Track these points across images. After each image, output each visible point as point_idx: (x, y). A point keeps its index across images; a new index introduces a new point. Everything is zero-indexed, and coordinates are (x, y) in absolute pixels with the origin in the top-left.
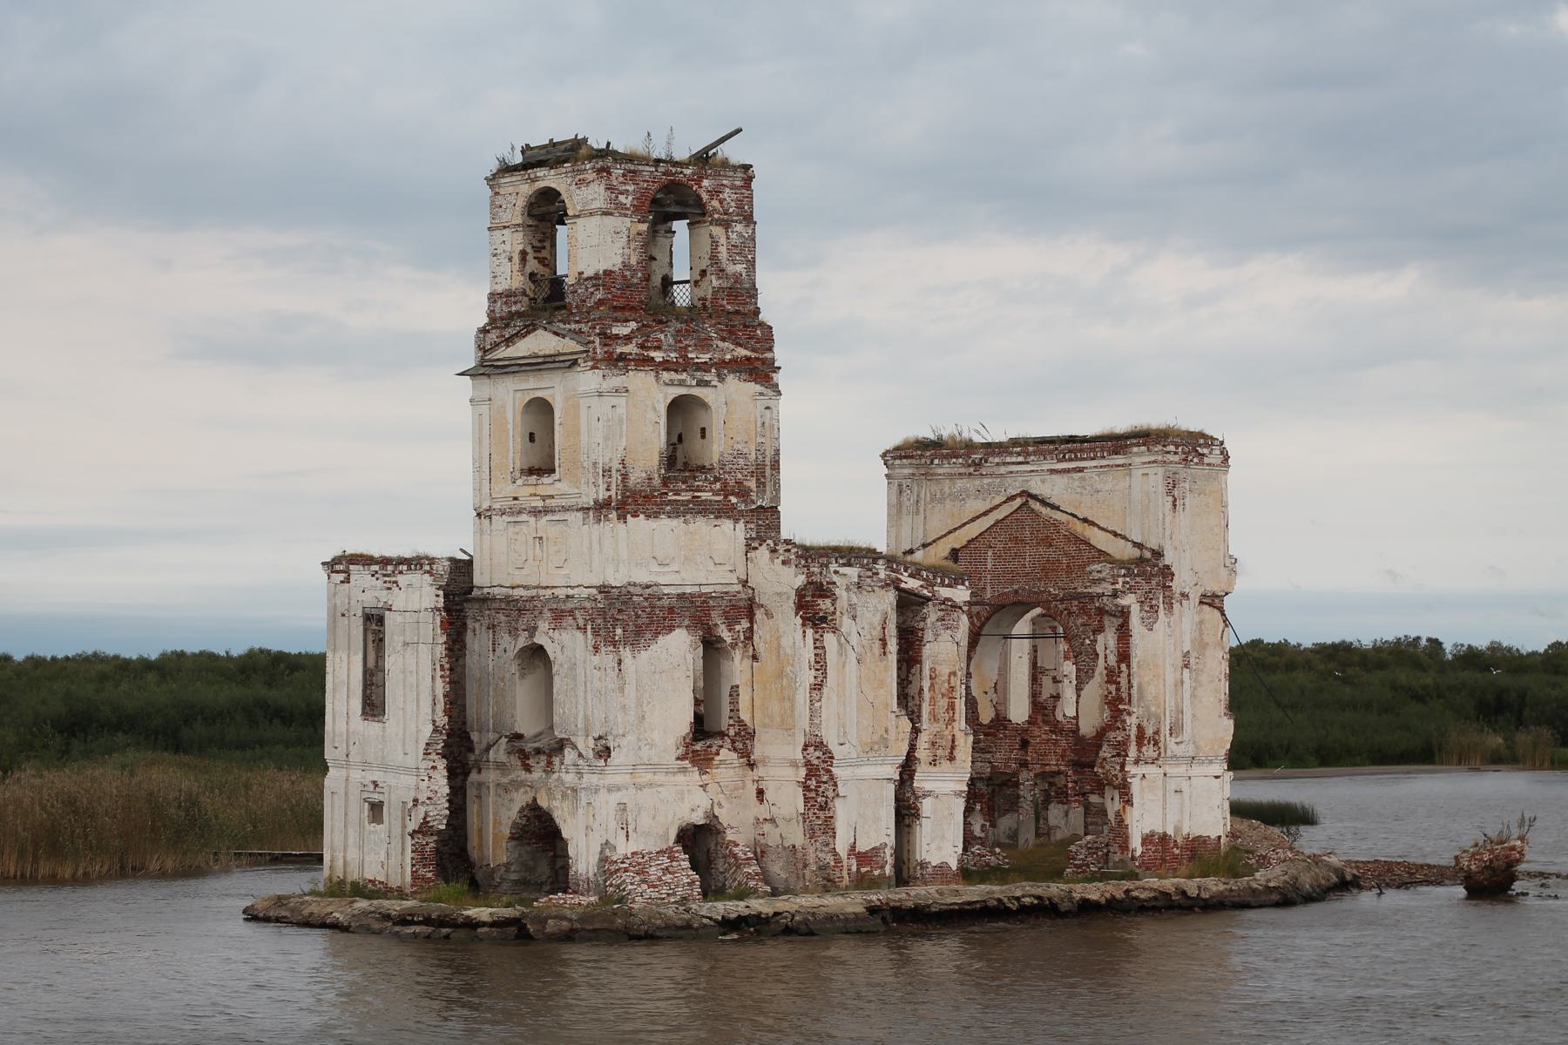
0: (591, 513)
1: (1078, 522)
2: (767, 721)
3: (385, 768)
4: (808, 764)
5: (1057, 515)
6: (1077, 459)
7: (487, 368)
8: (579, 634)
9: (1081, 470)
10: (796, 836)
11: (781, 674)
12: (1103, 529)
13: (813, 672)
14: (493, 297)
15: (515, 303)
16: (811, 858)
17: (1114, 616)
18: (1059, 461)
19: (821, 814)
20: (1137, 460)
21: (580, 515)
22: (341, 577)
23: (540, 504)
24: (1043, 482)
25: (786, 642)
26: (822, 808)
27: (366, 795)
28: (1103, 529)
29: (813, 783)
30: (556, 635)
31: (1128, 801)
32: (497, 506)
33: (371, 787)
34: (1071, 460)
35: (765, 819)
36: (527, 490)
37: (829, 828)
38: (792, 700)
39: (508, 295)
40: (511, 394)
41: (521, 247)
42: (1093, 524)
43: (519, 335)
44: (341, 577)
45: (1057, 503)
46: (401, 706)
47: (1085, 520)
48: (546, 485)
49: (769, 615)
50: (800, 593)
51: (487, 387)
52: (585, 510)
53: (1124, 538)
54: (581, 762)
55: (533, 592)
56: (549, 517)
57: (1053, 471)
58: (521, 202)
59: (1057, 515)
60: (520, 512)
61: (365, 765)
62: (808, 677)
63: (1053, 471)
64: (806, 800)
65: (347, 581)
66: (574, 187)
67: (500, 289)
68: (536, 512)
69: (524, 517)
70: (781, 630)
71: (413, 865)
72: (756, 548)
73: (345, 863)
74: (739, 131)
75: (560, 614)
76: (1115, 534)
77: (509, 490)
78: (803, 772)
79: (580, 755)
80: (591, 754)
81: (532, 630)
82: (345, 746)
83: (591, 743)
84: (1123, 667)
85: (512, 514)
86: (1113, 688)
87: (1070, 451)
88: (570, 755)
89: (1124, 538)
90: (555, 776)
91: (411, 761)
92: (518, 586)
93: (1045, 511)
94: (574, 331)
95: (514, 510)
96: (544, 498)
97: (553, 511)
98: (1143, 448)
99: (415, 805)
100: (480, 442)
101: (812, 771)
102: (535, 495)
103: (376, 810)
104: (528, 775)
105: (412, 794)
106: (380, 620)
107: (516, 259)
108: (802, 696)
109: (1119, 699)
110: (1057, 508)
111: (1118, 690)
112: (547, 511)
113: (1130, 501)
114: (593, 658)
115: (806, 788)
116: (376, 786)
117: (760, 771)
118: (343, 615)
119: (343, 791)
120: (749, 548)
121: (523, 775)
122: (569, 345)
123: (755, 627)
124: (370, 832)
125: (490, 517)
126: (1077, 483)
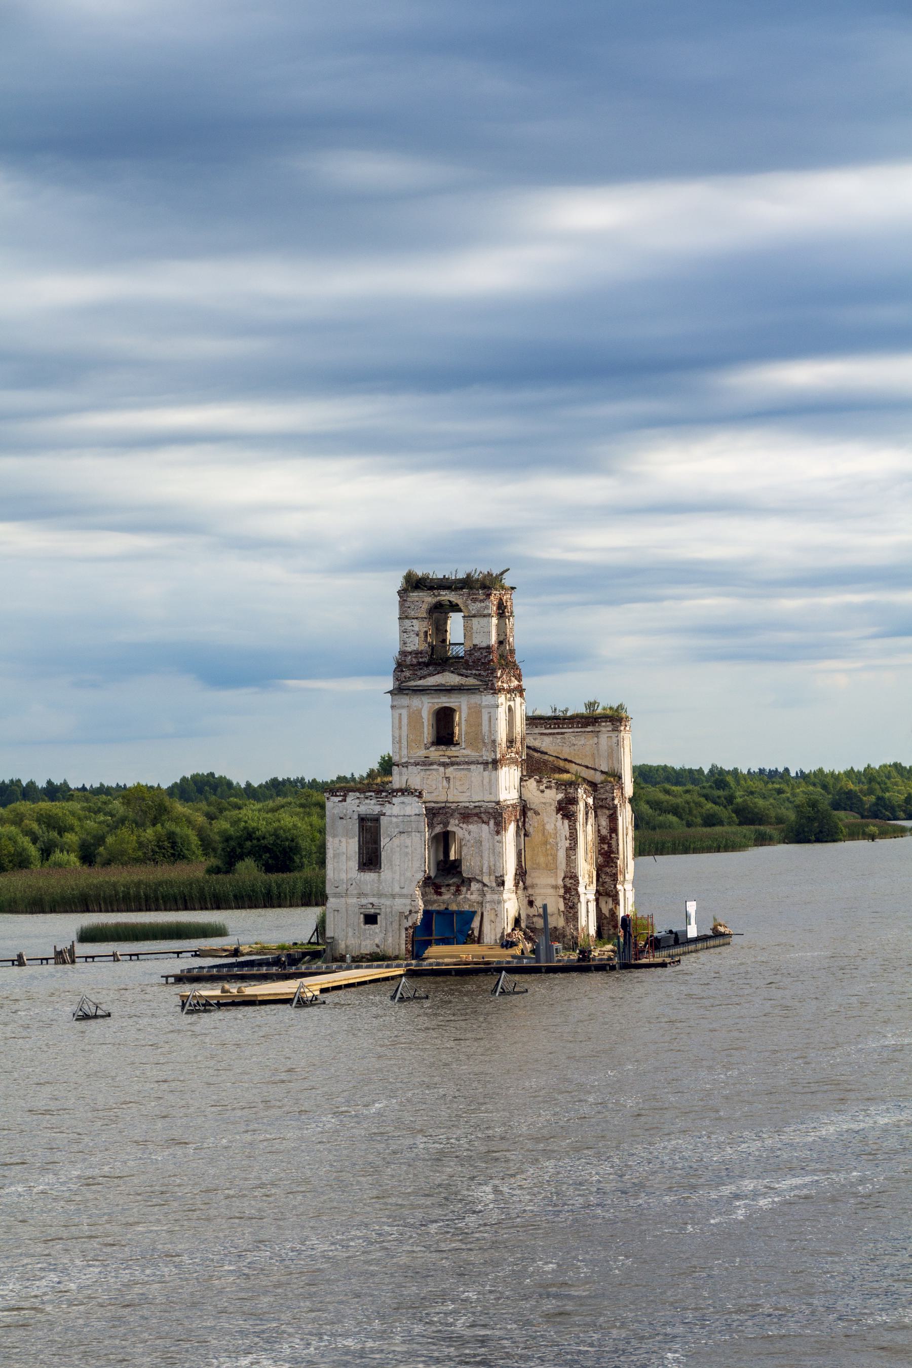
0: (490, 766)
1: (561, 761)
2: (535, 866)
3: (380, 895)
4: (565, 886)
5: (546, 757)
6: (559, 728)
7: (399, 690)
8: (484, 826)
9: (562, 734)
10: (561, 922)
11: (546, 843)
12: (578, 764)
13: (568, 841)
14: (403, 653)
15: (421, 657)
16: (568, 932)
17: (609, 809)
18: (546, 728)
19: (571, 911)
20: (603, 729)
21: (481, 767)
22: (340, 798)
23: (447, 760)
24: (535, 739)
25: (549, 827)
26: (570, 908)
27: (362, 910)
28: (578, 764)
29: (568, 896)
30: (464, 826)
31: (616, 902)
32: (412, 761)
33: (370, 906)
34: (555, 728)
35: (534, 916)
36: (435, 753)
37: (575, 918)
38: (555, 857)
39: (417, 653)
40: (426, 706)
41: (425, 629)
42: (571, 761)
43: (430, 675)
44: (340, 798)
45: (545, 751)
46: (398, 863)
47: (566, 760)
48: (453, 751)
49: (537, 813)
50: (560, 802)
51: (404, 700)
52: (486, 764)
53: (595, 770)
54: (486, 889)
55: (443, 805)
56: (456, 767)
57: (542, 734)
58: (425, 607)
59: (546, 757)
60: (432, 764)
61: (361, 895)
62: (567, 844)
63: (542, 734)
64: (565, 904)
65: (345, 800)
66: (470, 602)
67: (409, 649)
68: (444, 765)
69: (435, 767)
70: (545, 821)
71: (406, 944)
72: (526, 780)
73: (347, 947)
74: (509, 569)
75: (467, 815)
76: (587, 767)
77: (423, 752)
78: (562, 891)
79: (485, 885)
80: (494, 884)
81: (446, 824)
82: (345, 886)
83: (493, 878)
84: (614, 835)
85: (425, 765)
86: (606, 847)
87: (555, 724)
88: (475, 886)
89: (595, 770)
90: (462, 897)
91: (405, 891)
92: (430, 802)
93: (536, 754)
94: (475, 674)
95: (426, 763)
96: (449, 757)
97: (458, 764)
98: (608, 723)
99: (410, 914)
100: (400, 728)
101: (567, 890)
102: (444, 755)
103: (371, 919)
104: (439, 897)
105: (409, 908)
106: (376, 819)
107: (422, 635)
108: (562, 854)
109: (613, 852)
110: (546, 753)
111: (610, 846)
112: (452, 764)
113: (598, 750)
114: (496, 837)
115: (565, 899)
116: (373, 905)
117: (530, 891)
118: (341, 818)
119: (344, 909)
120: (521, 780)
121: (435, 897)
122: (471, 681)
123: (527, 820)
124: (365, 930)
125: (407, 767)
126: (559, 740)
